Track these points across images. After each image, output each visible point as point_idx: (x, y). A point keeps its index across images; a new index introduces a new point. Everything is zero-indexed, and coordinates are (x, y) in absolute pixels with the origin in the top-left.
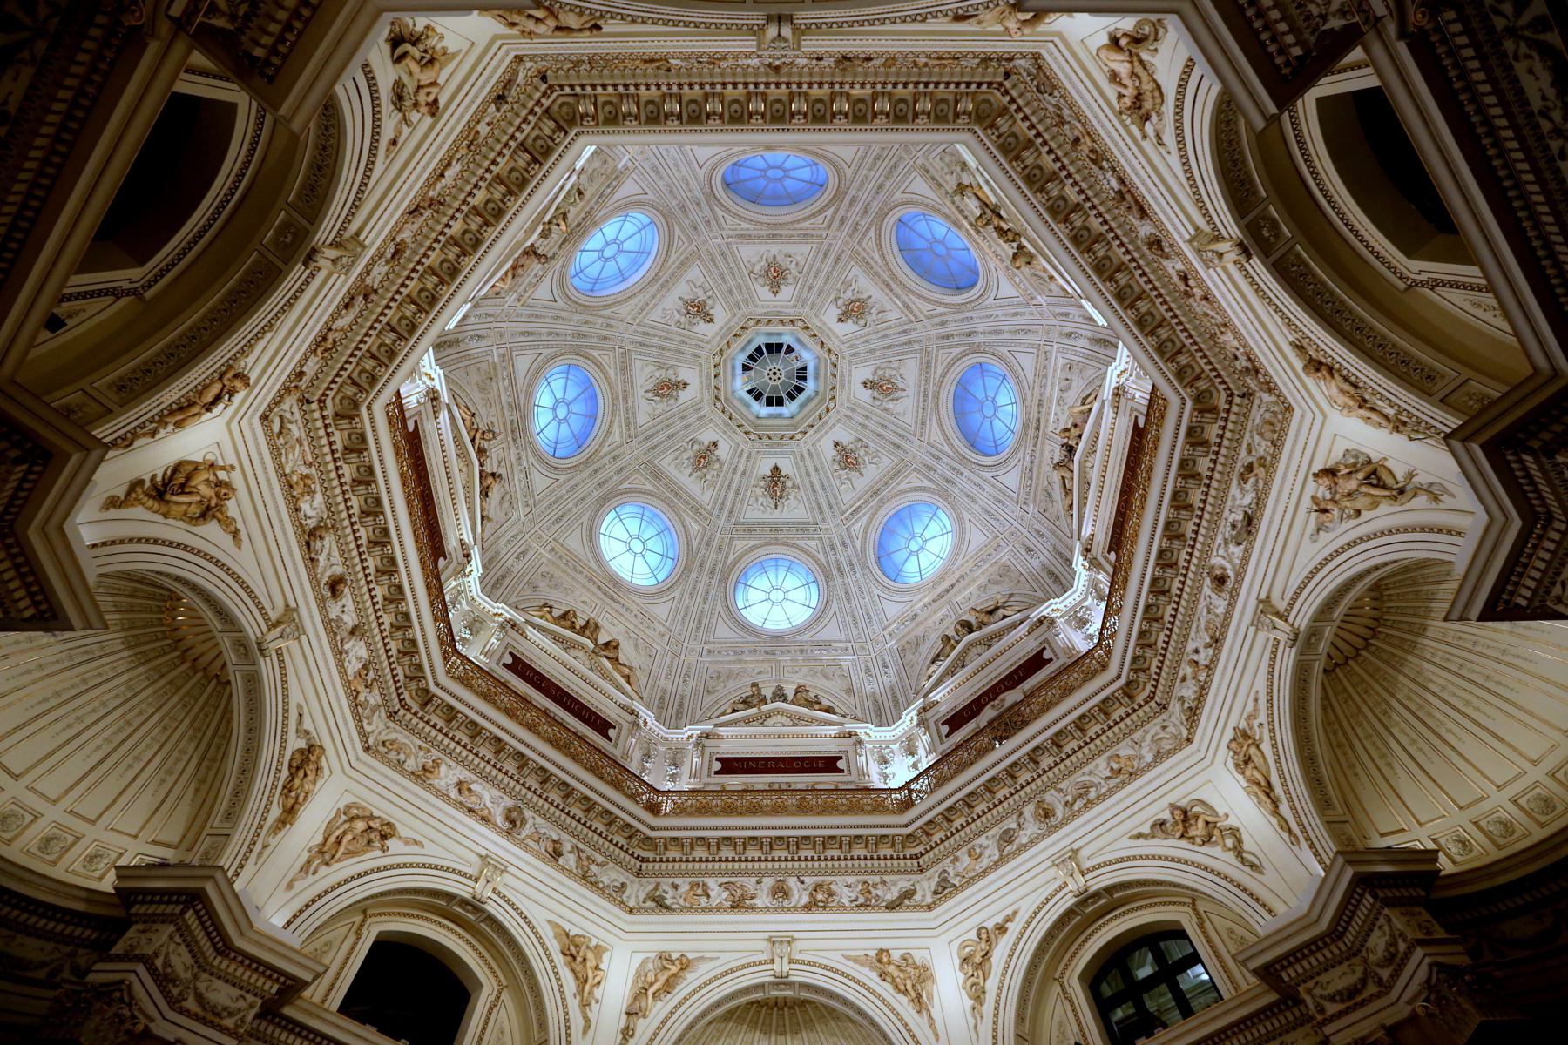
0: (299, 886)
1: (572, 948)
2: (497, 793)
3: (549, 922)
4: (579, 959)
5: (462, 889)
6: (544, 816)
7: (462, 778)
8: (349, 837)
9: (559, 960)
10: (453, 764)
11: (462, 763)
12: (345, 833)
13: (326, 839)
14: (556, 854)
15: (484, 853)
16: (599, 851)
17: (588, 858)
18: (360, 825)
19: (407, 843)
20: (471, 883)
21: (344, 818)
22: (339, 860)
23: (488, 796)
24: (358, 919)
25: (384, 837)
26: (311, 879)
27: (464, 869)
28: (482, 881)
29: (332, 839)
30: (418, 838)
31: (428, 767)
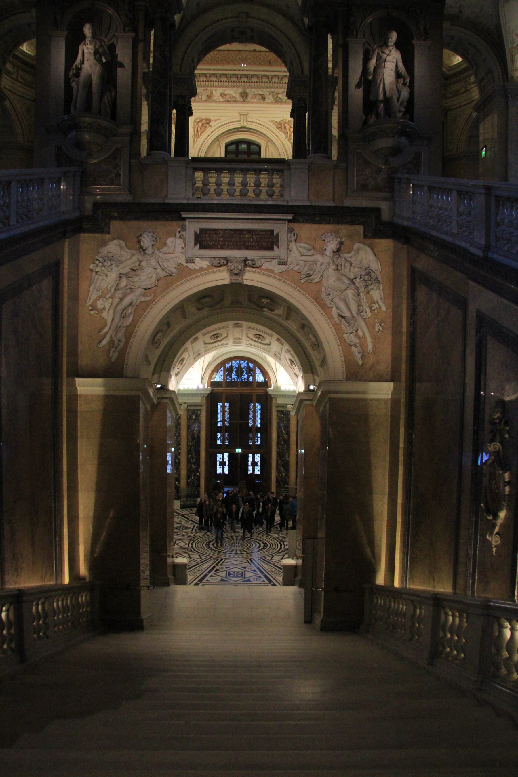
0: (195, 146)
1: (280, 126)
2: (235, 89)
3: (269, 121)
4: (283, 128)
5: (238, 125)
6: (254, 87)
7: (221, 92)
8: (199, 129)
9: (277, 131)
10: (216, 89)
11: (218, 86)
12: (198, 128)
13: (194, 132)
14: (264, 98)
15: (238, 111)
16: (279, 88)
17: (276, 94)
18: (200, 124)
19: (215, 121)
20: (240, 122)
21: (195, 124)
22: (201, 135)
23: (231, 92)
24: (218, 143)
25: (208, 123)
26: (197, 143)
27: (235, 120)
28: (242, 121)
29: (196, 131)
30: (218, 118)
31: (209, 95)
